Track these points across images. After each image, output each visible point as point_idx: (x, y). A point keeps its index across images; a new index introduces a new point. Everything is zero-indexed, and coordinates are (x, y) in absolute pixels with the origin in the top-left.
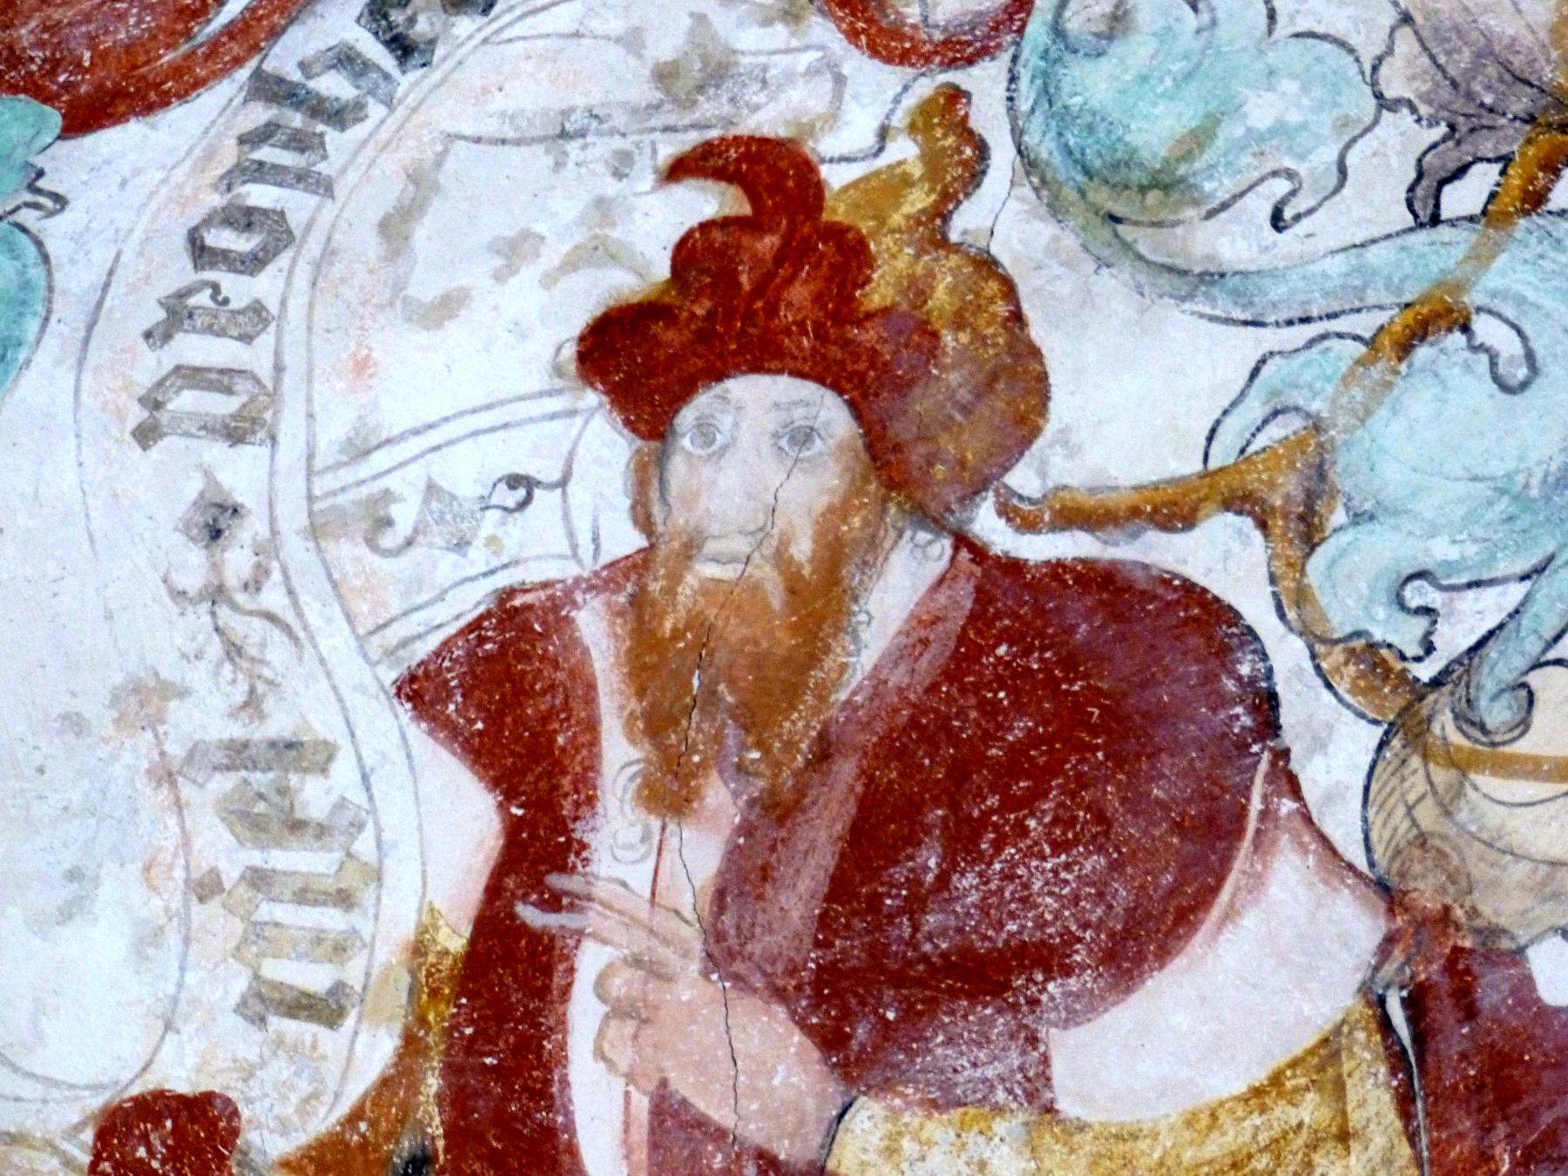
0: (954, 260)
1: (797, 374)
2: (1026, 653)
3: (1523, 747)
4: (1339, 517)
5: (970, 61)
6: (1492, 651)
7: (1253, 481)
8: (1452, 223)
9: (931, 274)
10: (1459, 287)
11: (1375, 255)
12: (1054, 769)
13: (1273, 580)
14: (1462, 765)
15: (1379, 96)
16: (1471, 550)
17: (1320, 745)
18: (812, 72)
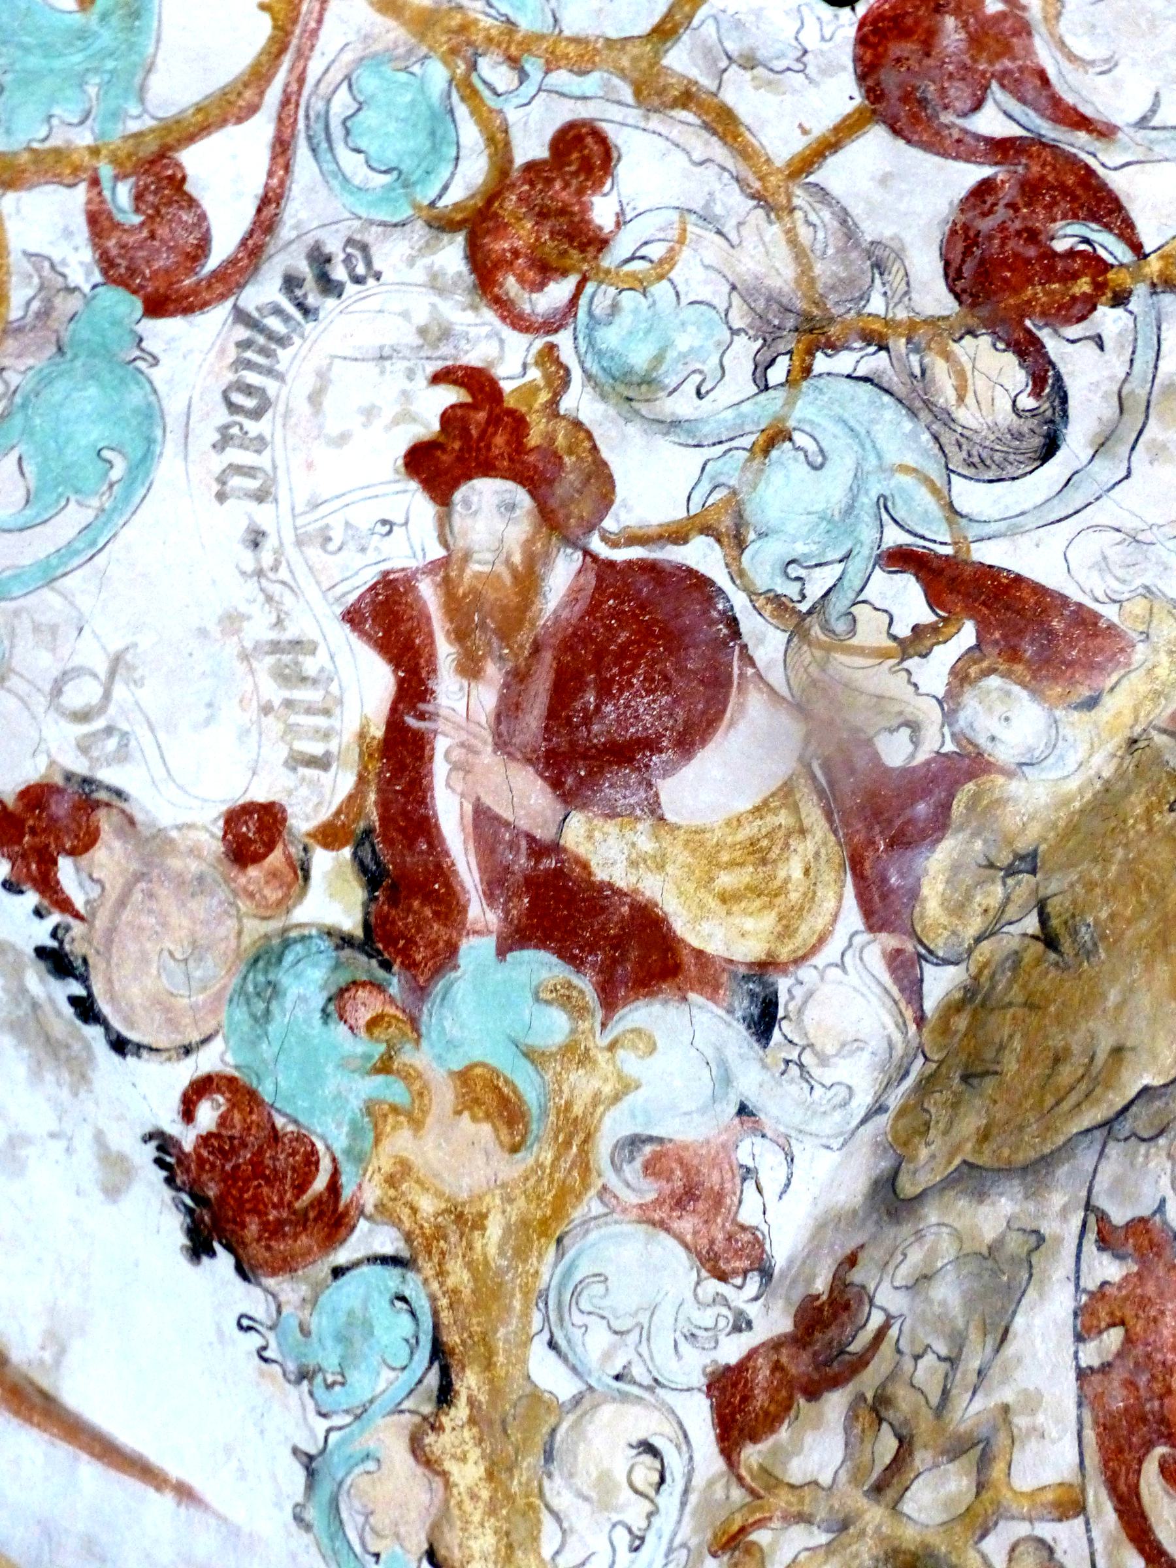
0: (564, 423)
1: (503, 477)
2: (623, 603)
3: (854, 641)
4: (752, 536)
5: (556, 331)
6: (833, 596)
7: (711, 519)
8: (775, 387)
9: (555, 430)
10: (783, 419)
11: (746, 407)
12: (641, 655)
13: (727, 566)
14: (828, 649)
15: (730, 328)
16: (814, 547)
17: (761, 641)
18: (488, 337)
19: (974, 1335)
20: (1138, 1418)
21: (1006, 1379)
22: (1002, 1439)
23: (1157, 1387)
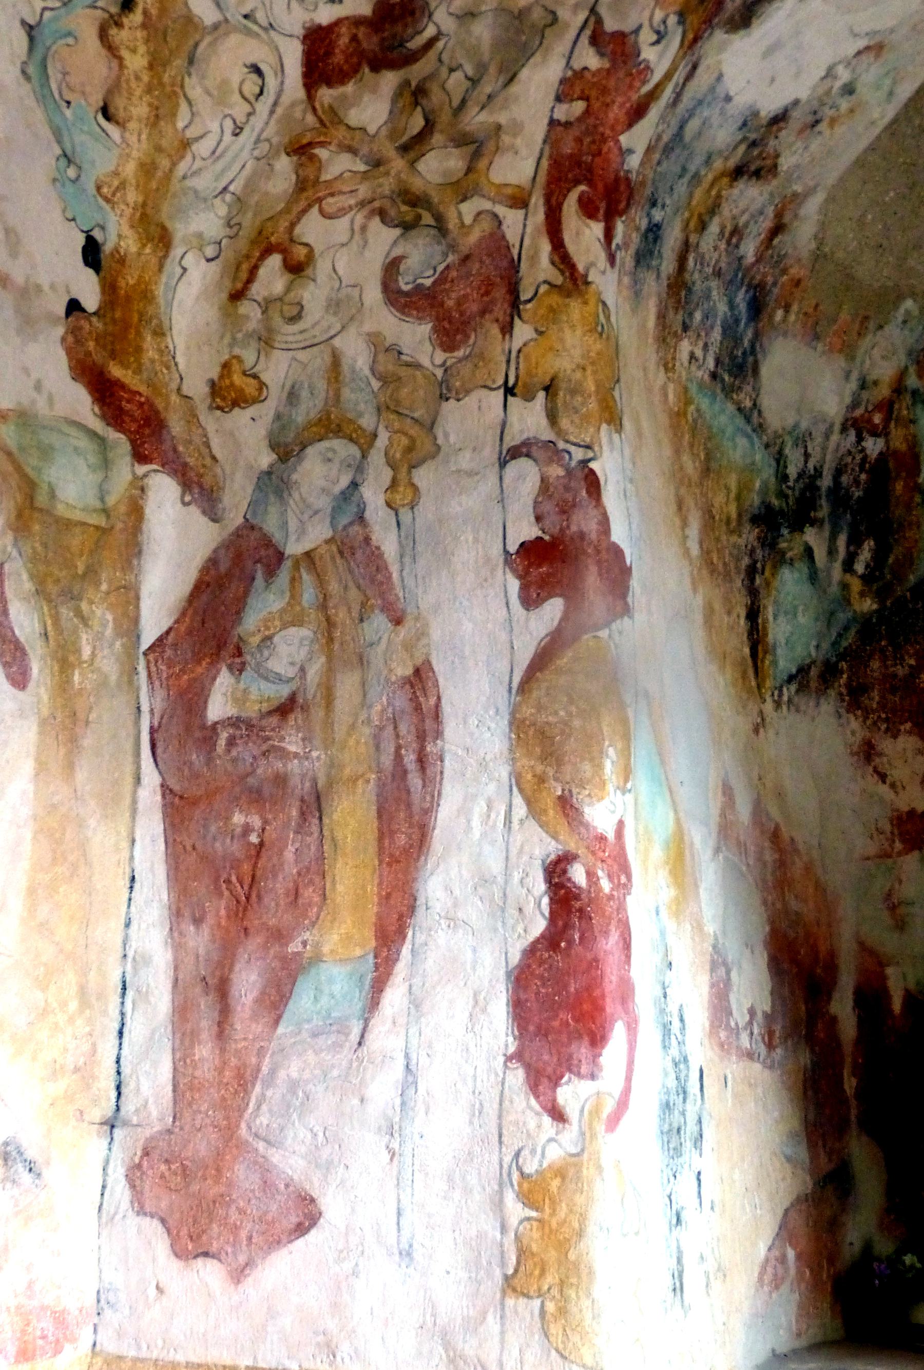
19: (492, 70)
20: (575, 161)
21: (504, 107)
22: (491, 145)
23: (594, 147)
